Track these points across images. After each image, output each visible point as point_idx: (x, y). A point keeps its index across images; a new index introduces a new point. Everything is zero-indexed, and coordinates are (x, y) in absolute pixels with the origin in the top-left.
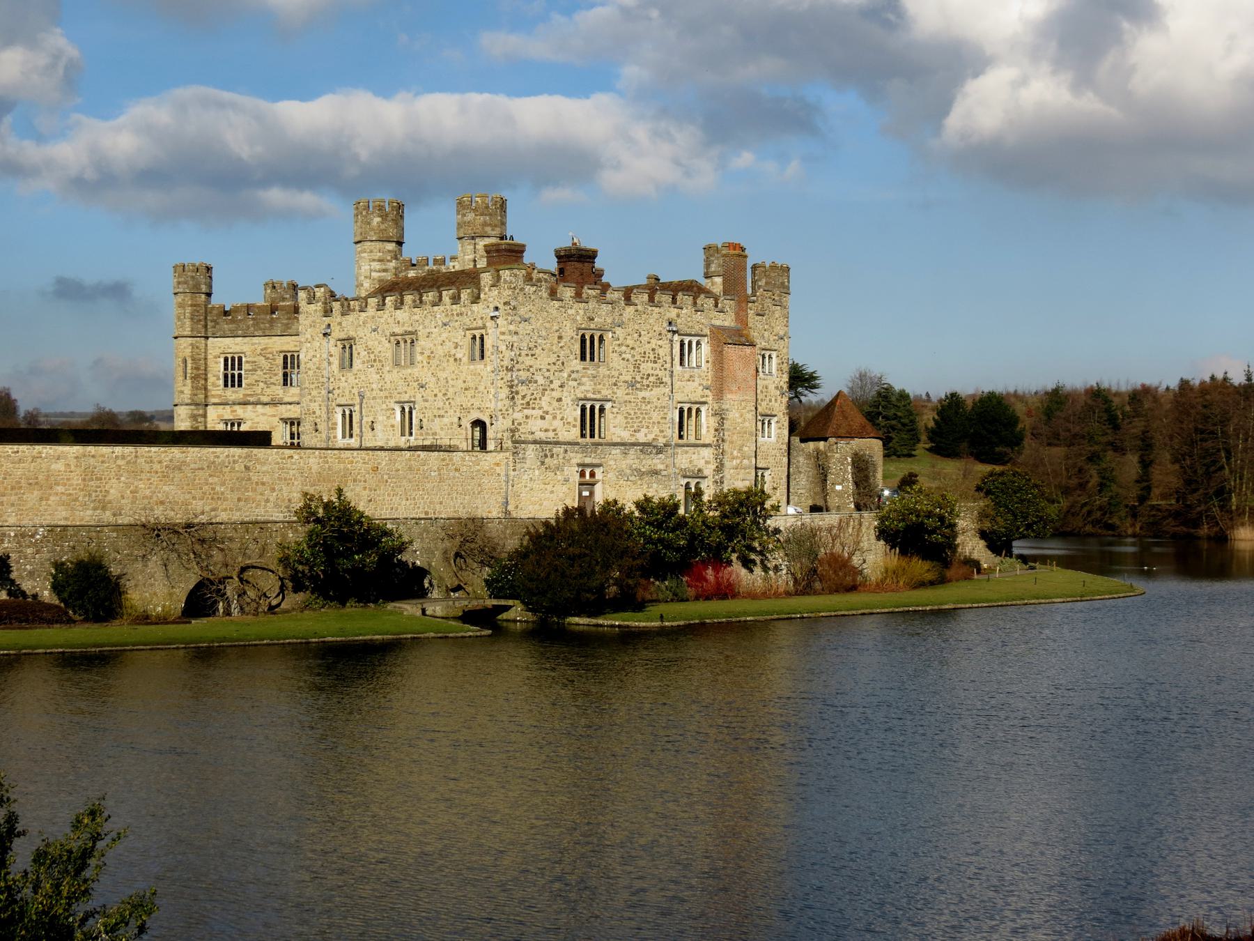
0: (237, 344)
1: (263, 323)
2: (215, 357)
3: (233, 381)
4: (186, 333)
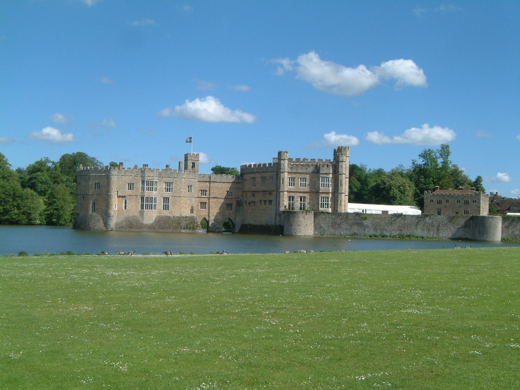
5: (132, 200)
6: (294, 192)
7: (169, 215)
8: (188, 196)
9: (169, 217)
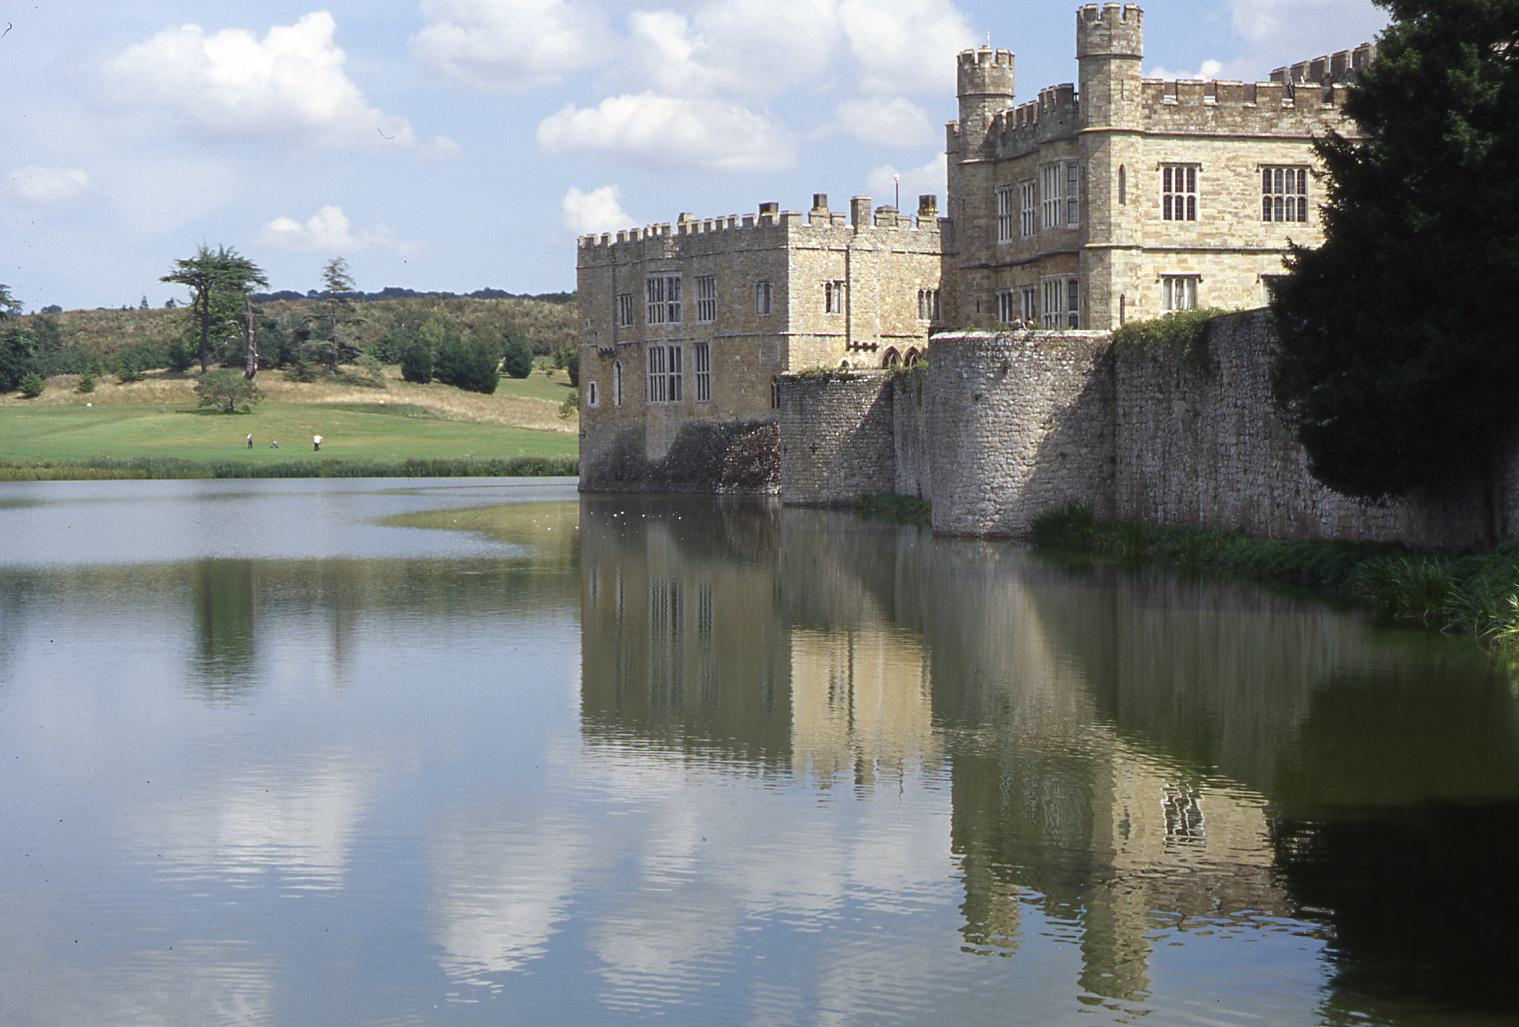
0: (1188, 148)
1: (1231, 115)
2: (1150, 169)
3: (1179, 210)
4: (1125, 126)
5: (633, 364)
6: (1012, 265)
7: (710, 420)
8: (760, 333)
9: (706, 429)
